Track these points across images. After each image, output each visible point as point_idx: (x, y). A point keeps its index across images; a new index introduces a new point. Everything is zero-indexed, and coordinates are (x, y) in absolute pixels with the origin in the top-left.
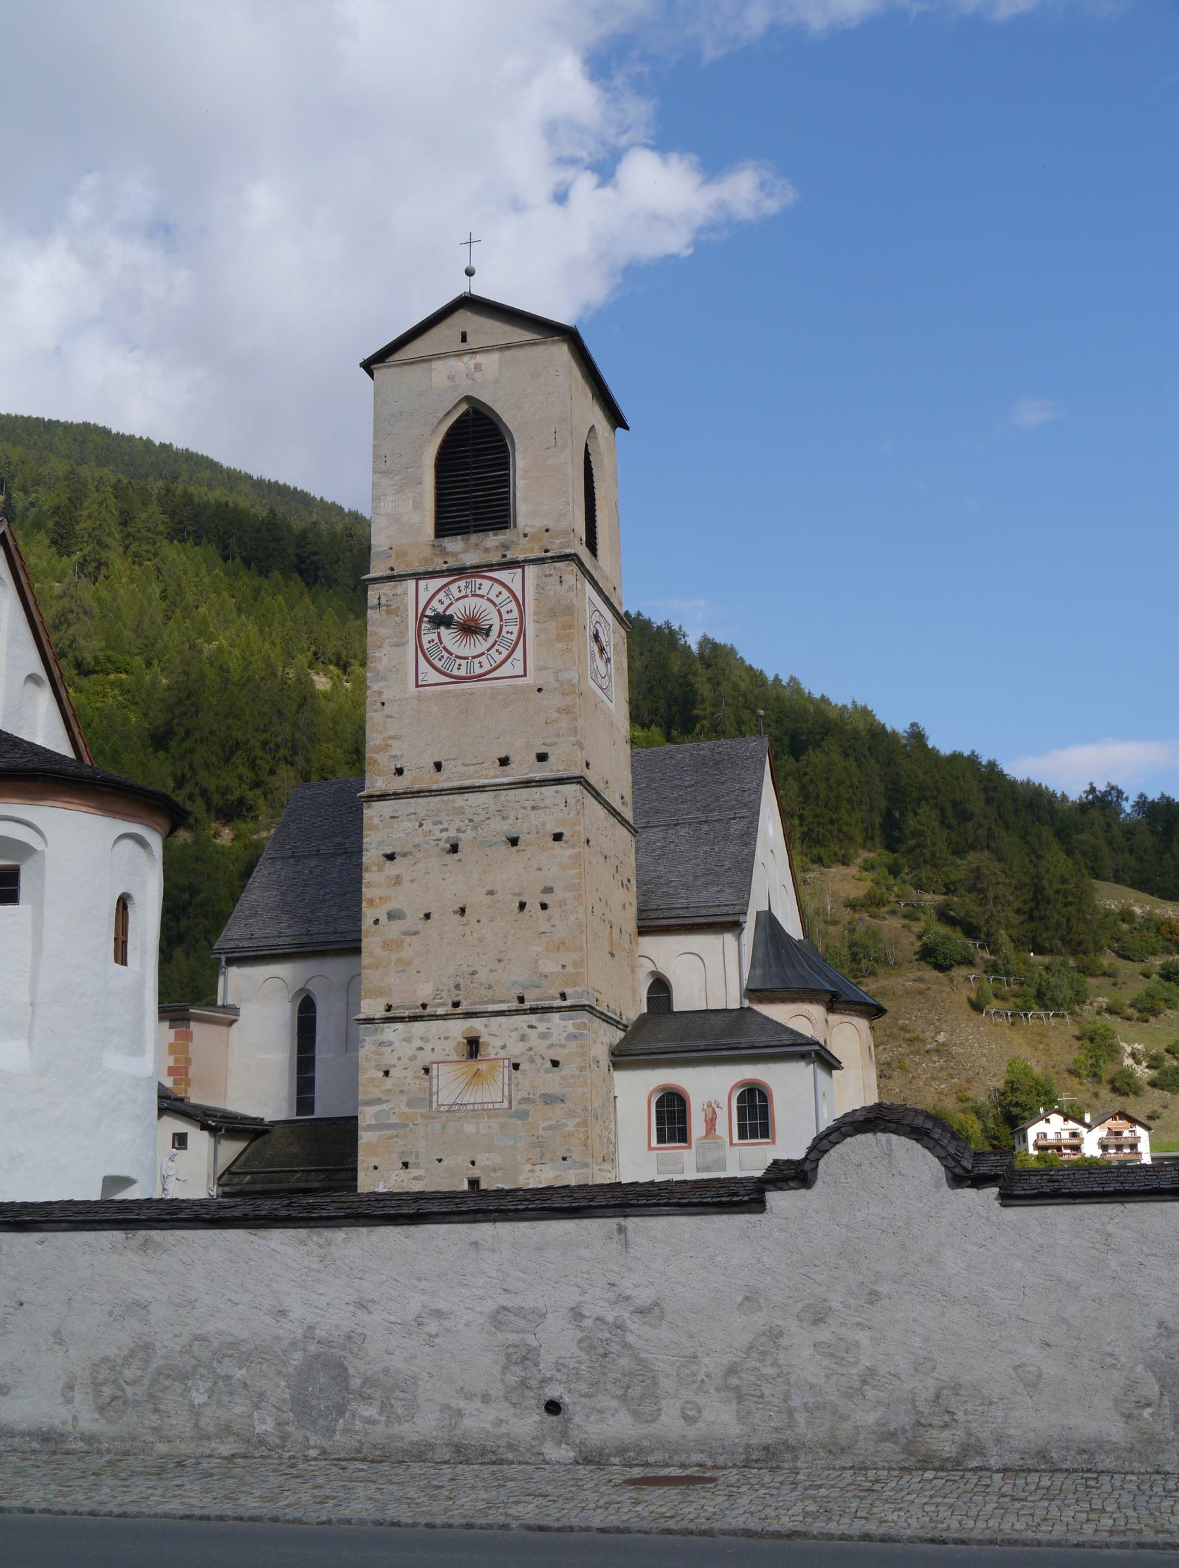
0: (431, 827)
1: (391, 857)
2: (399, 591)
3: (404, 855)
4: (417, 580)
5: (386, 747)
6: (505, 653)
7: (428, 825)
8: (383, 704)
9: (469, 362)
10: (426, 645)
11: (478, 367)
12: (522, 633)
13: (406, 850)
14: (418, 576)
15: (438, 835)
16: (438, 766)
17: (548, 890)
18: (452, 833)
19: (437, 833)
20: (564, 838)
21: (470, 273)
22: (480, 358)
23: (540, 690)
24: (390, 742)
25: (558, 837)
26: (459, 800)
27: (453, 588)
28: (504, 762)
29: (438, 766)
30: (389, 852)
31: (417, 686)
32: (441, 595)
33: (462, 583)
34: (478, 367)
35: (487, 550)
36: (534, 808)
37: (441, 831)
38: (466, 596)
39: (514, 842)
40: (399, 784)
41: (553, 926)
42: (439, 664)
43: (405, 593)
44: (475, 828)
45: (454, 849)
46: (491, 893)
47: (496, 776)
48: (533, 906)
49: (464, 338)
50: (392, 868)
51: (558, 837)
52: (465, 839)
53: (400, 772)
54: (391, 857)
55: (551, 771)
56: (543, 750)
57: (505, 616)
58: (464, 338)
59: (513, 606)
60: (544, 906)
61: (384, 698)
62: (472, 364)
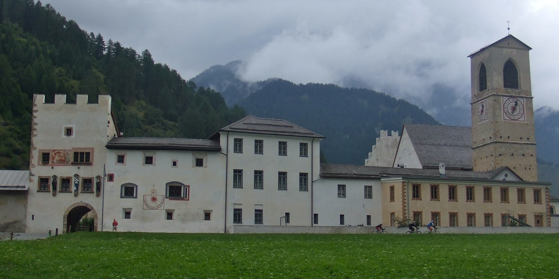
0: (508, 150)
1: (500, 155)
2: (499, 98)
3: (503, 155)
4: (503, 97)
5: (499, 132)
6: (521, 116)
7: (508, 150)
8: (497, 122)
9: (510, 50)
10: (505, 111)
11: (512, 51)
12: (524, 112)
13: (503, 154)
14: (503, 96)
15: (509, 152)
16: (508, 137)
17: (530, 166)
18: (512, 152)
19: (509, 151)
20: (533, 156)
21: (509, 29)
22: (512, 50)
23: (527, 125)
24: (499, 131)
25: (532, 155)
26: (513, 145)
27: (510, 100)
28: (521, 138)
29: (508, 137)
30: (500, 154)
31: (504, 120)
32: (508, 101)
33: (512, 99)
34: (512, 51)
35: (516, 93)
36: (527, 149)
37: (510, 151)
38: (512, 102)
39: (523, 155)
40: (501, 140)
41: (532, 173)
42: (508, 116)
43: (501, 99)
44: (516, 151)
45: (512, 155)
46: (520, 165)
47: (520, 141)
48: (527, 168)
49: (508, 44)
50: (501, 157)
51: (532, 155)
52: (515, 153)
53: (501, 137)
54: (500, 155)
55: (530, 142)
56: (528, 137)
57: (520, 108)
58: (508, 44)
59: (522, 106)
60: (530, 169)
61: (498, 121)
62: (511, 50)
